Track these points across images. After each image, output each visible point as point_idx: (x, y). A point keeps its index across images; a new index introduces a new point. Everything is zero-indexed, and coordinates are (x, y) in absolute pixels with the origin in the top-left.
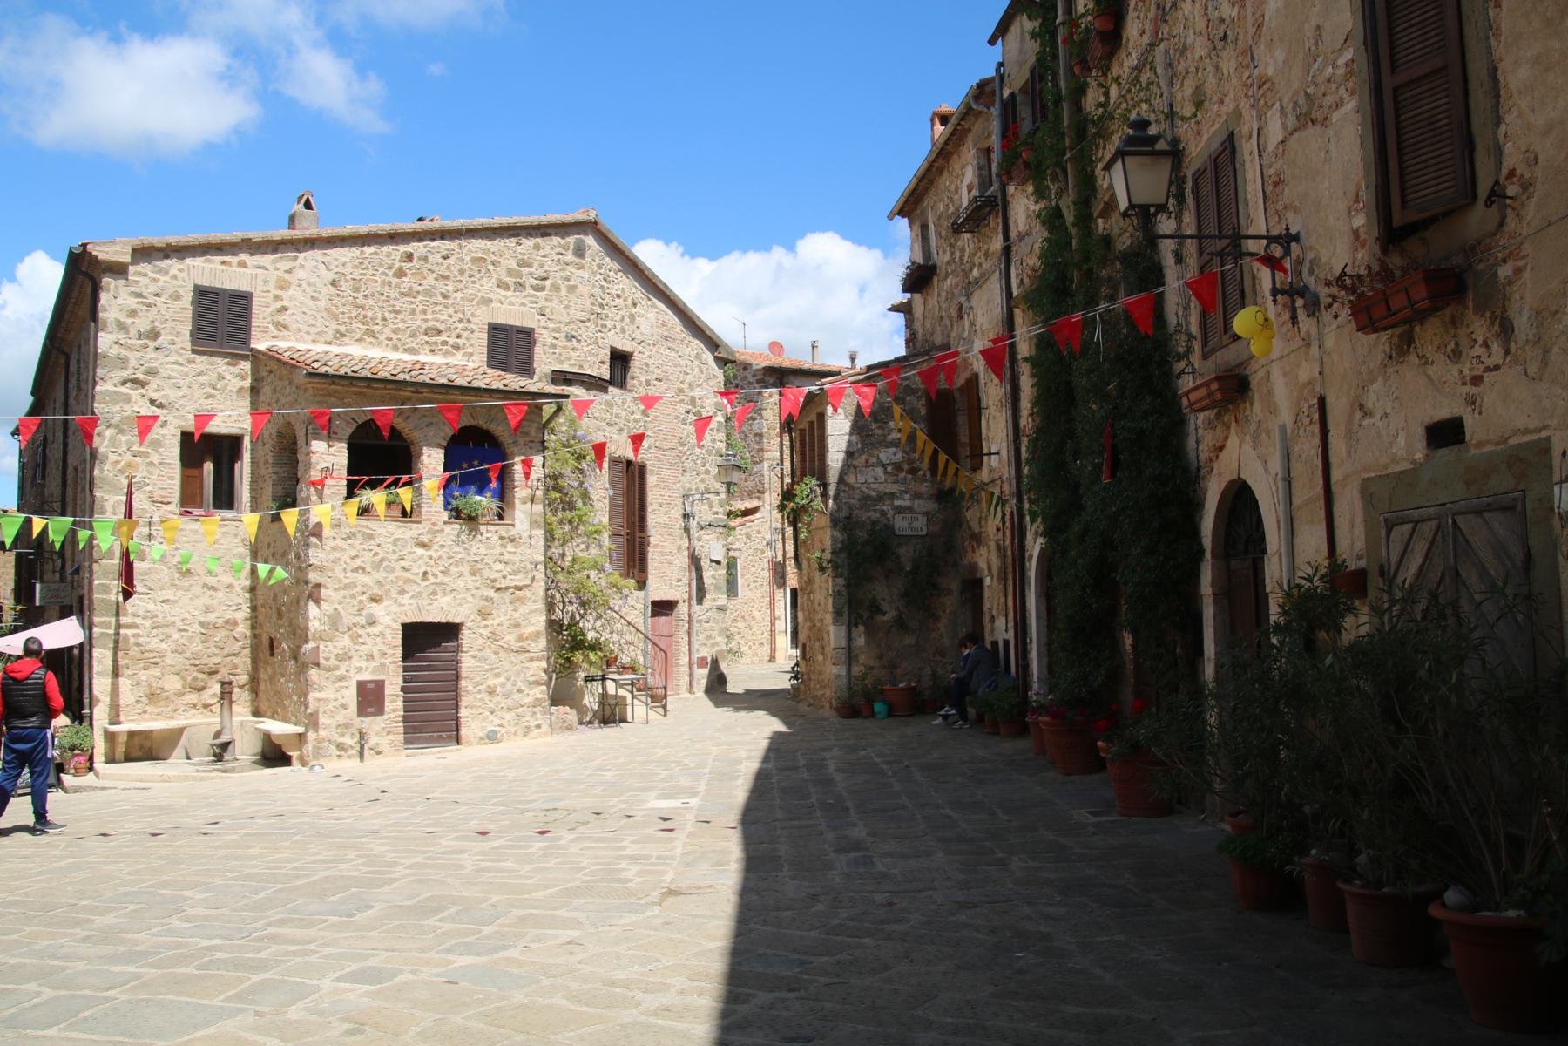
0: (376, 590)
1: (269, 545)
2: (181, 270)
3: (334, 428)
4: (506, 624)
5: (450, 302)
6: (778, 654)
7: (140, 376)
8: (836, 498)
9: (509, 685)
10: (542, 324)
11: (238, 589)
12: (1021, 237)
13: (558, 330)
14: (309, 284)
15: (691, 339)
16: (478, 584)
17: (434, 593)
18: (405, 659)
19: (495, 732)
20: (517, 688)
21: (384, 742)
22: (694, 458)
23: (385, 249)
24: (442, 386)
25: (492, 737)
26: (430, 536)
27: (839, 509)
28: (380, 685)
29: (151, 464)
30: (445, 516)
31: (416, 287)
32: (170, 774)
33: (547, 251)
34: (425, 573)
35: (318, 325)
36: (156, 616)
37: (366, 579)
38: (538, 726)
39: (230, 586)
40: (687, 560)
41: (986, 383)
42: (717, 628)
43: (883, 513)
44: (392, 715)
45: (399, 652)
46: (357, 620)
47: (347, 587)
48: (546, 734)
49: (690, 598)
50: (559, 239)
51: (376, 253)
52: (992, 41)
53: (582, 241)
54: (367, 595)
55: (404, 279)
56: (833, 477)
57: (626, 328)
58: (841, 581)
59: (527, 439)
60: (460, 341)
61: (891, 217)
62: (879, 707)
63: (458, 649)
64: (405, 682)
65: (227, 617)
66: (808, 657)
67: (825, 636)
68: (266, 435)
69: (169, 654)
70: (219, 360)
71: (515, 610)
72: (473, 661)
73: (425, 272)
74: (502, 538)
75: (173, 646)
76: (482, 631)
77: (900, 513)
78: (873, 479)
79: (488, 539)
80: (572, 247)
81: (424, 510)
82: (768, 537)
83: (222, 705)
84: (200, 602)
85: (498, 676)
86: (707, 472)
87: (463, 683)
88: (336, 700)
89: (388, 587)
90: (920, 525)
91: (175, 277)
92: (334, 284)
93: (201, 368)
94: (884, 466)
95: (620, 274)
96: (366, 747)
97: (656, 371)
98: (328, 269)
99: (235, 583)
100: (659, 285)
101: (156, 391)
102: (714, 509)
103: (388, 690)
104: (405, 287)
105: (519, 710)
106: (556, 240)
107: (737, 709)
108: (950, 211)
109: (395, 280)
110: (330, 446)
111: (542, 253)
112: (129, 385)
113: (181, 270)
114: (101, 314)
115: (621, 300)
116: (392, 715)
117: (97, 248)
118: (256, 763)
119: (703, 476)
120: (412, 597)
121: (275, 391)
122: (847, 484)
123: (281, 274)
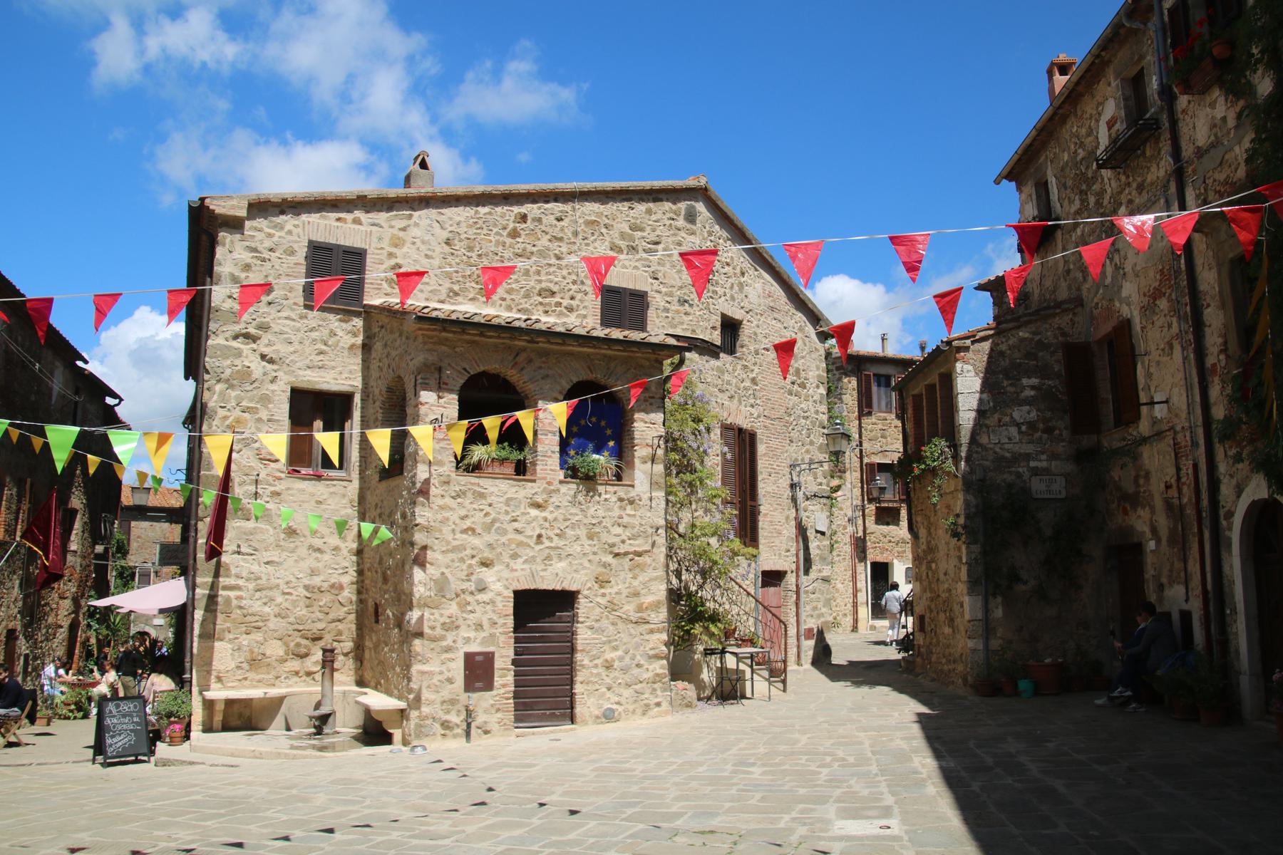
0: (487, 554)
1: (376, 505)
2: (296, 226)
3: (444, 378)
4: (625, 592)
5: (563, 263)
6: (860, 625)
7: (252, 330)
8: (968, 460)
9: (627, 660)
10: (655, 287)
11: (345, 552)
12: (1200, 153)
13: (671, 295)
14: (423, 242)
15: (795, 311)
16: (595, 549)
17: (549, 558)
18: (516, 630)
19: (612, 711)
20: (636, 662)
21: (493, 720)
22: (800, 429)
23: (499, 209)
24: (560, 334)
25: (609, 716)
26: (545, 496)
27: (972, 471)
28: (489, 658)
29: (260, 420)
30: (561, 475)
31: (529, 248)
32: (262, 749)
33: (659, 216)
34: (540, 536)
35: (431, 283)
36: (260, 578)
37: (476, 541)
38: (658, 704)
39: (336, 549)
40: (794, 530)
41: (1143, 328)
42: (822, 599)
43: (1019, 475)
44: (502, 691)
45: (510, 621)
46: (465, 585)
47: (455, 549)
48: (666, 713)
49: (798, 568)
50: (670, 204)
51: (490, 213)
53: (693, 207)
54: (476, 559)
55: (518, 239)
56: (964, 437)
57: (736, 296)
58: (976, 548)
59: (647, 395)
60: (574, 303)
61: (997, 182)
62: (1023, 685)
63: (573, 619)
64: (516, 654)
65: (333, 581)
66: (928, 628)
67: (956, 608)
68: (377, 391)
69: (272, 618)
70: (331, 316)
71: (634, 578)
72: (589, 633)
73: (539, 233)
74: (621, 500)
75: (277, 610)
76: (599, 599)
77: (1036, 475)
78: (1008, 439)
79: (606, 500)
80: (683, 213)
81: (538, 468)
82: (850, 514)
83: (323, 673)
84: (305, 565)
85: (615, 648)
86: (812, 443)
87: (578, 656)
88: (441, 673)
89: (499, 550)
90: (1059, 488)
91: (290, 232)
92: (448, 242)
93: (313, 324)
94: (1018, 425)
95: (729, 242)
96: (473, 725)
97: (763, 340)
98: (442, 228)
99: (342, 545)
100: (765, 255)
101: (267, 345)
102: (819, 480)
103: (498, 664)
104: (519, 248)
105: (638, 687)
106: (667, 205)
107: (858, 684)
108: (1079, 158)
109: (509, 241)
110: (440, 397)
111: (654, 217)
112: (241, 339)
113: (296, 226)
114: (215, 268)
115: (730, 268)
116: (502, 691)
117: (215, 202)
118: (356, 738)
119: (808, 447)
120: (526, 561)
121: (386, 345)
122: (981, 445)
123: (395, 231)
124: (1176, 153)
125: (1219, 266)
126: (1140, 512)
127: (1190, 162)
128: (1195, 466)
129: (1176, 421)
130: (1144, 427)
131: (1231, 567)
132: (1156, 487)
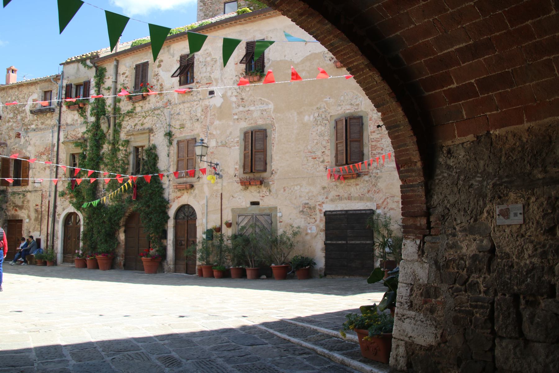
52: (61, 64)
124: (59, 121)
125: (67, 154)
126: (23, 211)
127: (63, 125)
128: (49, 202)
129: (43, 188)
130: (29, 187)
131: (58, 227)
132: (32, 205)
